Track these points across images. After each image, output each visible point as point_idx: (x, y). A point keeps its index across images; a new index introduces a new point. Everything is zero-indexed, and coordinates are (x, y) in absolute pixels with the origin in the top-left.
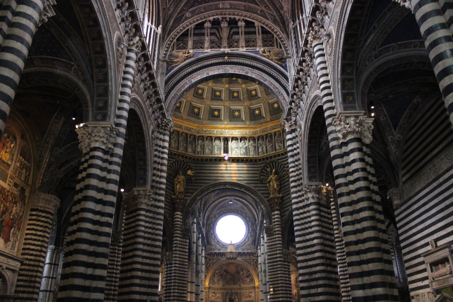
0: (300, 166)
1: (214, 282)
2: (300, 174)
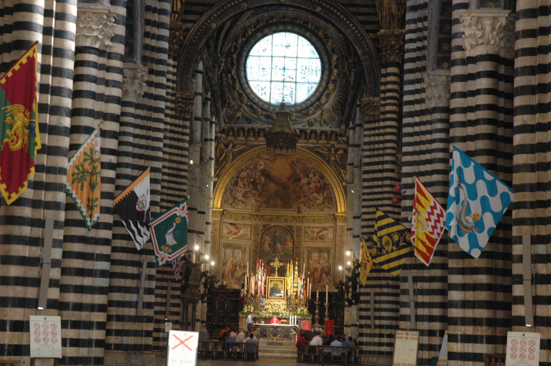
0: (426, 33)
1: (235, 198)
2: (424, 48)
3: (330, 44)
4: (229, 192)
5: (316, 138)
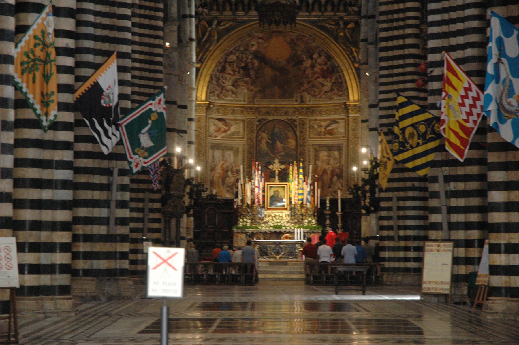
1: (223, 88)
4: (215, 80)
5: (320, 10)
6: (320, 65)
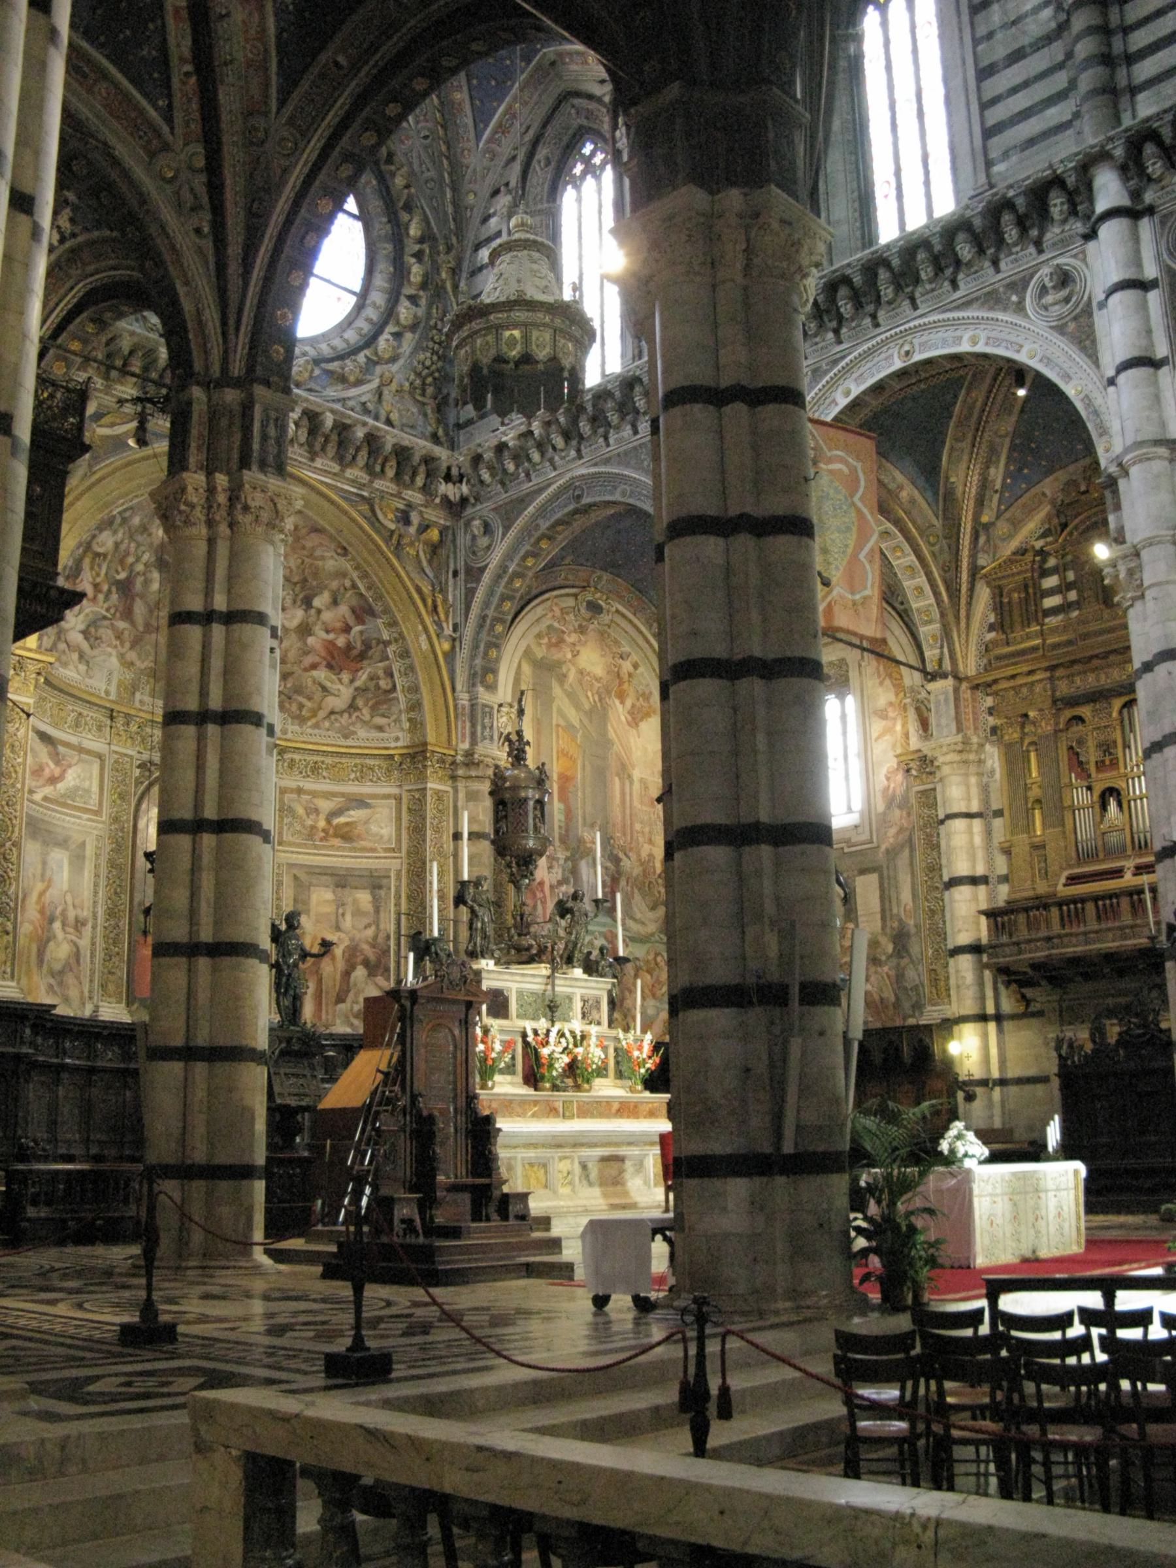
3: (399, 181)
5: (368, 468)
6: (328, 632)
